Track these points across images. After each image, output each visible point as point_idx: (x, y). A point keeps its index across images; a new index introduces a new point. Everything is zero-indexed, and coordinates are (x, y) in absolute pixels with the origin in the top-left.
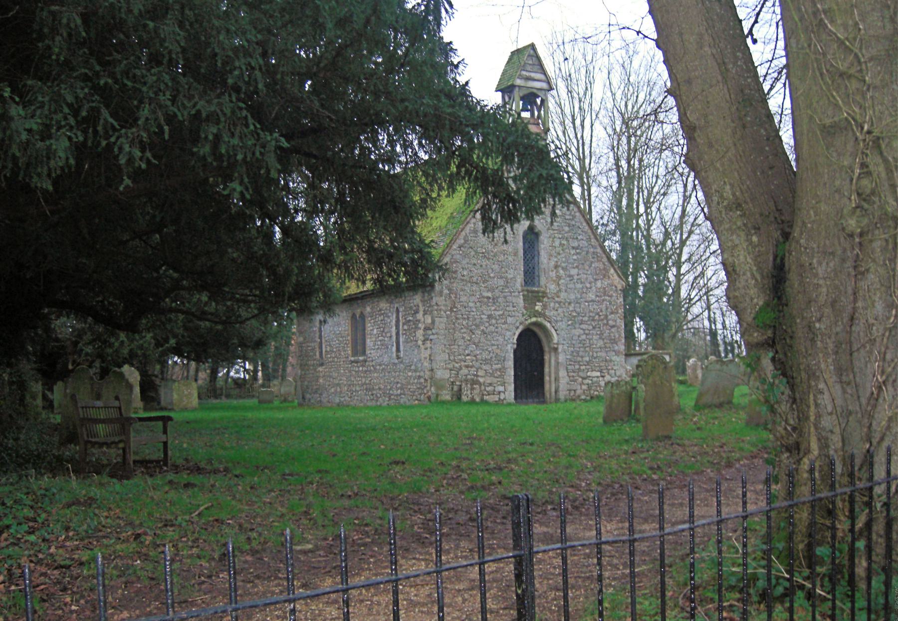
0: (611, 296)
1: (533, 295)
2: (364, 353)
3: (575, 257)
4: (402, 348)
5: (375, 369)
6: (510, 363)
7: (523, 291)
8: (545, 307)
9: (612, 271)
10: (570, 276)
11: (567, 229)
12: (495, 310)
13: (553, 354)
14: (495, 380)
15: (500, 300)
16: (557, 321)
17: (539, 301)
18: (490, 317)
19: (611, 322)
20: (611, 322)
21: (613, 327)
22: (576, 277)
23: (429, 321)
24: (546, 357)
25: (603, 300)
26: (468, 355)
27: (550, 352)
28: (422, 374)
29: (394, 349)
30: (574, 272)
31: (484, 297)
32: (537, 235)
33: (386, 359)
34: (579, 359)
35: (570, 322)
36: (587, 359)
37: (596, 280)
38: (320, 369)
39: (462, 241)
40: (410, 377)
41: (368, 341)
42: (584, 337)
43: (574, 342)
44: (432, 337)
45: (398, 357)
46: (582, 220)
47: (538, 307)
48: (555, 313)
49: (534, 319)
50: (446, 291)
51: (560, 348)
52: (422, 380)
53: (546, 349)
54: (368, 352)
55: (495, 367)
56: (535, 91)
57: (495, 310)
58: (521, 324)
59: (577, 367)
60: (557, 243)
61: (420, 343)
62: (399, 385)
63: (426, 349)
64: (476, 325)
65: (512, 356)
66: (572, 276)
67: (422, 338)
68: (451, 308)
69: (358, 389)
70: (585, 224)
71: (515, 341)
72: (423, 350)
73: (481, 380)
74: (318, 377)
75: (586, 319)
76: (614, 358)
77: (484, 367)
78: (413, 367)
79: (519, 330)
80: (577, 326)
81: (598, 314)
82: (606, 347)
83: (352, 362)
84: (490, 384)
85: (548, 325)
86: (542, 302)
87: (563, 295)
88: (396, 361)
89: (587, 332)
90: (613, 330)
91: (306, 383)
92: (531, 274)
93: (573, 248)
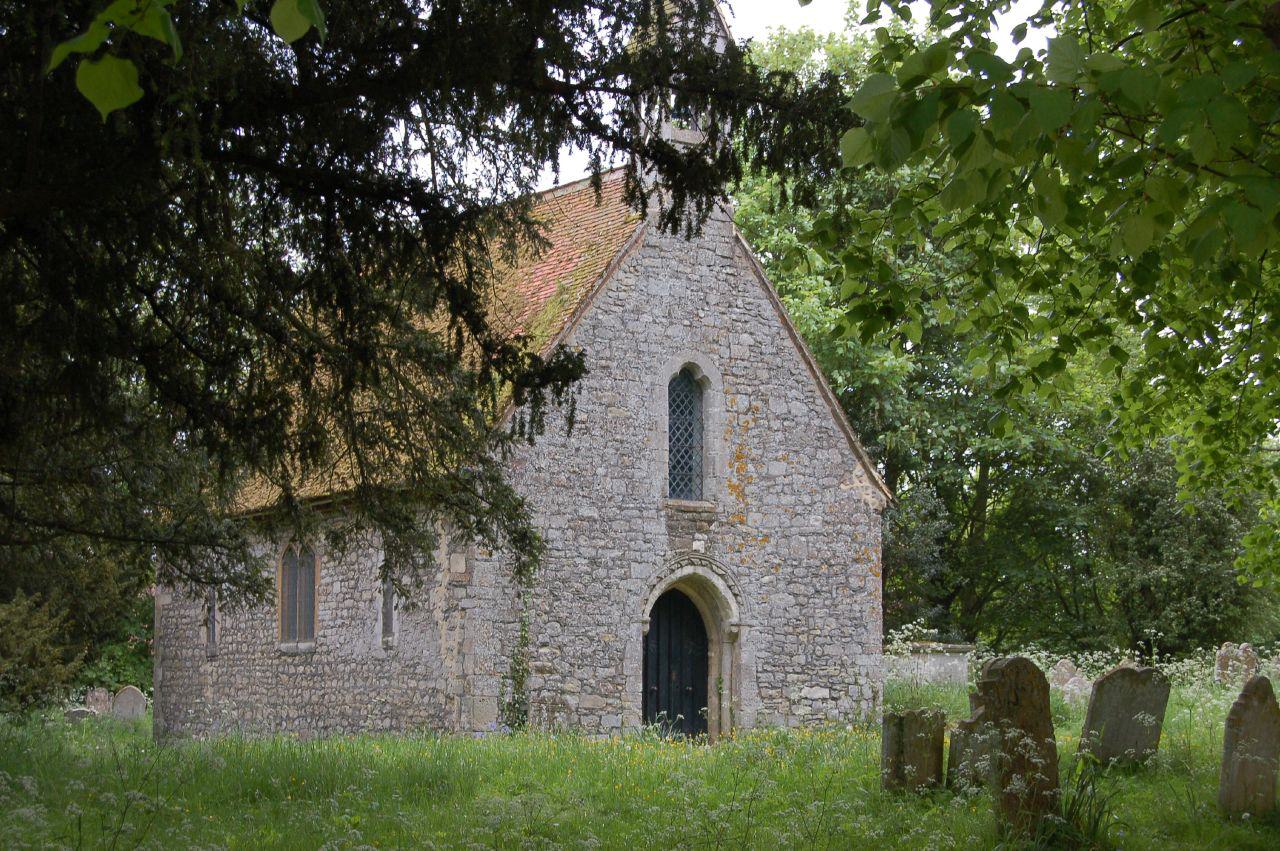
1: (686, 523)
2: (309, 633)
4: (396, 626)
5: (335, 671)
6: (634, 665)
8: (711, 543)
9: (859, 470)
10: (768, 477)
11: (764, 375)
12: (603, 548)
13: (726, 648)
14: (602, 702)
15: (615, 525)
16: (738, 575)
17: (700, 530)
18: (594, 562)
19: (854, 582)
20: (854, 582)
21: (861, 589)
22: (780, 480)
23: (461, 567)
24: (711, 654)
26: (544, 645)
27: (720, 643)
28: (441, 685)
29: (379, 627)
30: (778, 469)
31: (582, 519)
33: (359, 648)
34: (785, 658)
36: (802, 659)
38: (208, 667)
40: (414, 689)
41: (321, 607)
43: (775, 622)
44: (464, 603)
45: (387, 647)
46: (797, 356)
47: (698, 545)
48: (736, 557)
49: (688, 570)
51: (745, 631)
52: (441, 699)
53: (713, 636)
54: (319, 633)
55: (602, 672)
59: (780, 676)
60: (743, 402)
61: (438, 615)
62: (388, 707)
63: (452, 629)
65: (640, 647)
66: (774, 478)
67: (443, 604)
69: (293, 714)
70: (803, 366)
71: (647, 617)
72: (444, 632)
73: (572, 701)
74: (202, 686)
77: (579, 673)
78: (420, 669)
79: (657, 593)
80: (782, 585)
81: (826, 562)
83: (284, 654)
84: (591, 711)
85: (719, 583)
86: (707, 532)
87: (754, 517)
88: (382, 655)
89: (801, 599)
90: (859, 597)
91: (173, 698)
92: (684, 473)
93: (777, 417)
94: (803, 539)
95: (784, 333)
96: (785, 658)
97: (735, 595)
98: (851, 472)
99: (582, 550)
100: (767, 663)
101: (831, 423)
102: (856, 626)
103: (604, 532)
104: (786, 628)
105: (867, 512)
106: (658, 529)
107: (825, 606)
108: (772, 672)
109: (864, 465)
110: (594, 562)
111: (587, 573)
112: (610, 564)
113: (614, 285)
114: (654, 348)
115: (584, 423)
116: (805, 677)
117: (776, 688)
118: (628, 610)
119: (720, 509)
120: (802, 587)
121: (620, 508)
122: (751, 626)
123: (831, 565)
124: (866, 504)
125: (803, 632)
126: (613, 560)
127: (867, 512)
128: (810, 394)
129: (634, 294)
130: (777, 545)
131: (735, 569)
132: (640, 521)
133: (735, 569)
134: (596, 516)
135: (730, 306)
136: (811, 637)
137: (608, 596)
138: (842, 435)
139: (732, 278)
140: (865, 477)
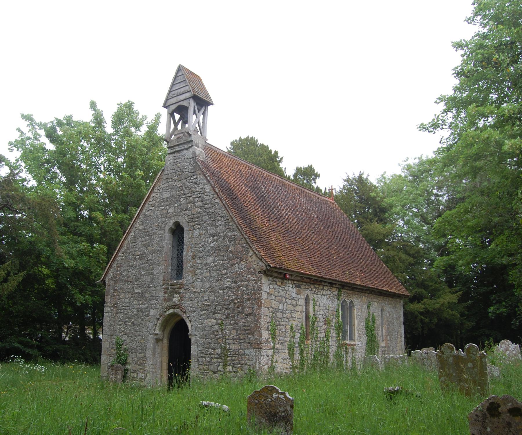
0: (249, 280)
3: (212, 245)
7: (164, 285)
10: (206, 265)
17: (177, 293)
18: (138, 310)
25: (239, 287)
30: (210, 260)
32: (182, 230)
34: (211, 351)
35: (203, 312)
36: (219, 351)
37: (233, 265)
39: (125, 248)
42: (216, 327)
47: (176, 300)
49: (171, 311)
50: (112, 291)
55: (139, 355)
56: (181, 103)
57: (142, 304)
58: (161, 316)
59: (209, 359)
64: (129, 318)
68: (114, 305)
75: (219, 307)
76: (246, 351)
80: (211, 315)
82: (239, 339)
86: (179, 293)
87: (199, 284)
89: (220, 322)
90: (249, 319)
94: (221, 291)
95: (215, 196)
96: (211, 351)
97: (190, 321)
98: (247, 254)
99: (135, 306)
100: (202, 353)
101: (236, 233)
102: (248, 334)
103: (142, 297)
104: (211, 336)
105: (255, 273)
106: (161, 295)
107: (230, 324)
108: (205, 357)
109: (253, 251)
110: (138, 310)
111: (136, 315)
112: (144, 310)
113: (151, 199)
114: (164, 219)
115: (138, 255)
116: (220, 360)
117: (207, 365)
118: (149, 329)
119: (185, 283)
120: (219, 315)
121: (148, 287)
122: (196, 335)
123: (235, 303)
124: (254, 270)
125: (220, 338)
126: (144, 308)
127: (255, 273)
128: (226, 221)
129: (158, 200)
130: (209, 296)
131: (190, 309)
132: (154, 292)
133: (190, 309)
134: (140, 291)
135: (194, 192)
136: (224, 340)
137: (142, 324)
138: (242, 237)
139: (194, 180)
140: (254, 256)
